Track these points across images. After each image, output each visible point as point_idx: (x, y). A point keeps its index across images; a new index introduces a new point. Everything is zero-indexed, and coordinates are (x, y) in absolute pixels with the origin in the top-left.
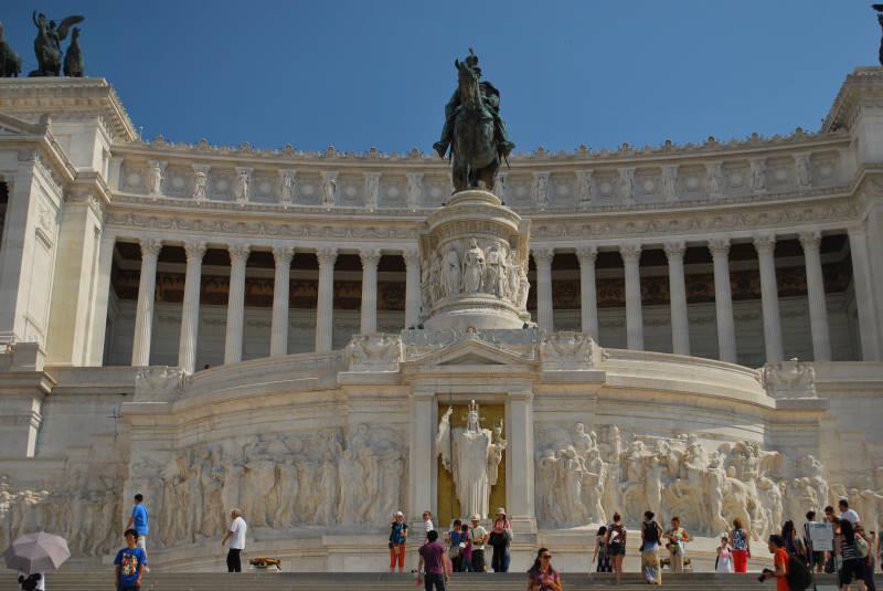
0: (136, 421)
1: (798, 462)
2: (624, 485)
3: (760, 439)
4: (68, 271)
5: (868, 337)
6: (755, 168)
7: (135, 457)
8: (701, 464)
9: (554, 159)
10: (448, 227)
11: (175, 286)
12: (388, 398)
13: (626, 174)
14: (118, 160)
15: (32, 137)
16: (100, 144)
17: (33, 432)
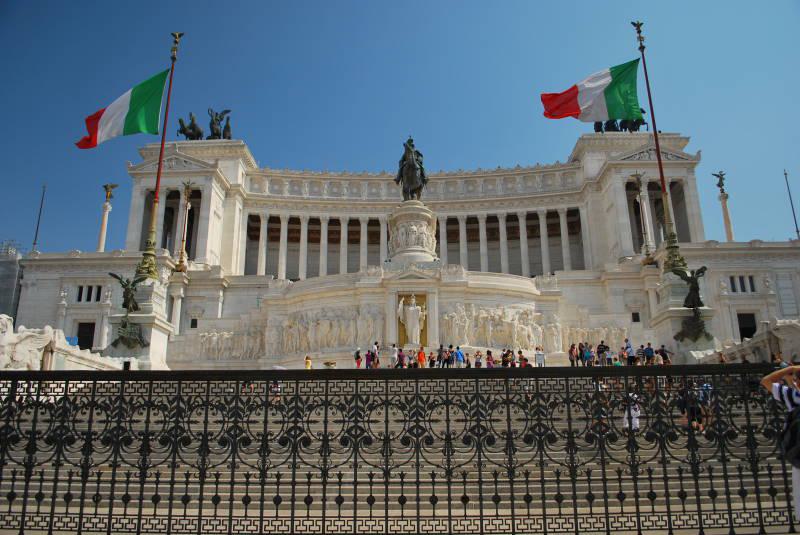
0: (271, 302)
1: (549, 318)
3: (533, 308)
4: (228, 229)
5: (587, 256)
6: (538, 179)
7: (270, 318)
8: (508, 320)
9: (447, 175)
10: (401, 216)
11: (276, 234)
12: (377, 293)
13: (480, 181)
14: (249, 178)
15: (211, 170)
16: (241, 170)
17: (220, 304)
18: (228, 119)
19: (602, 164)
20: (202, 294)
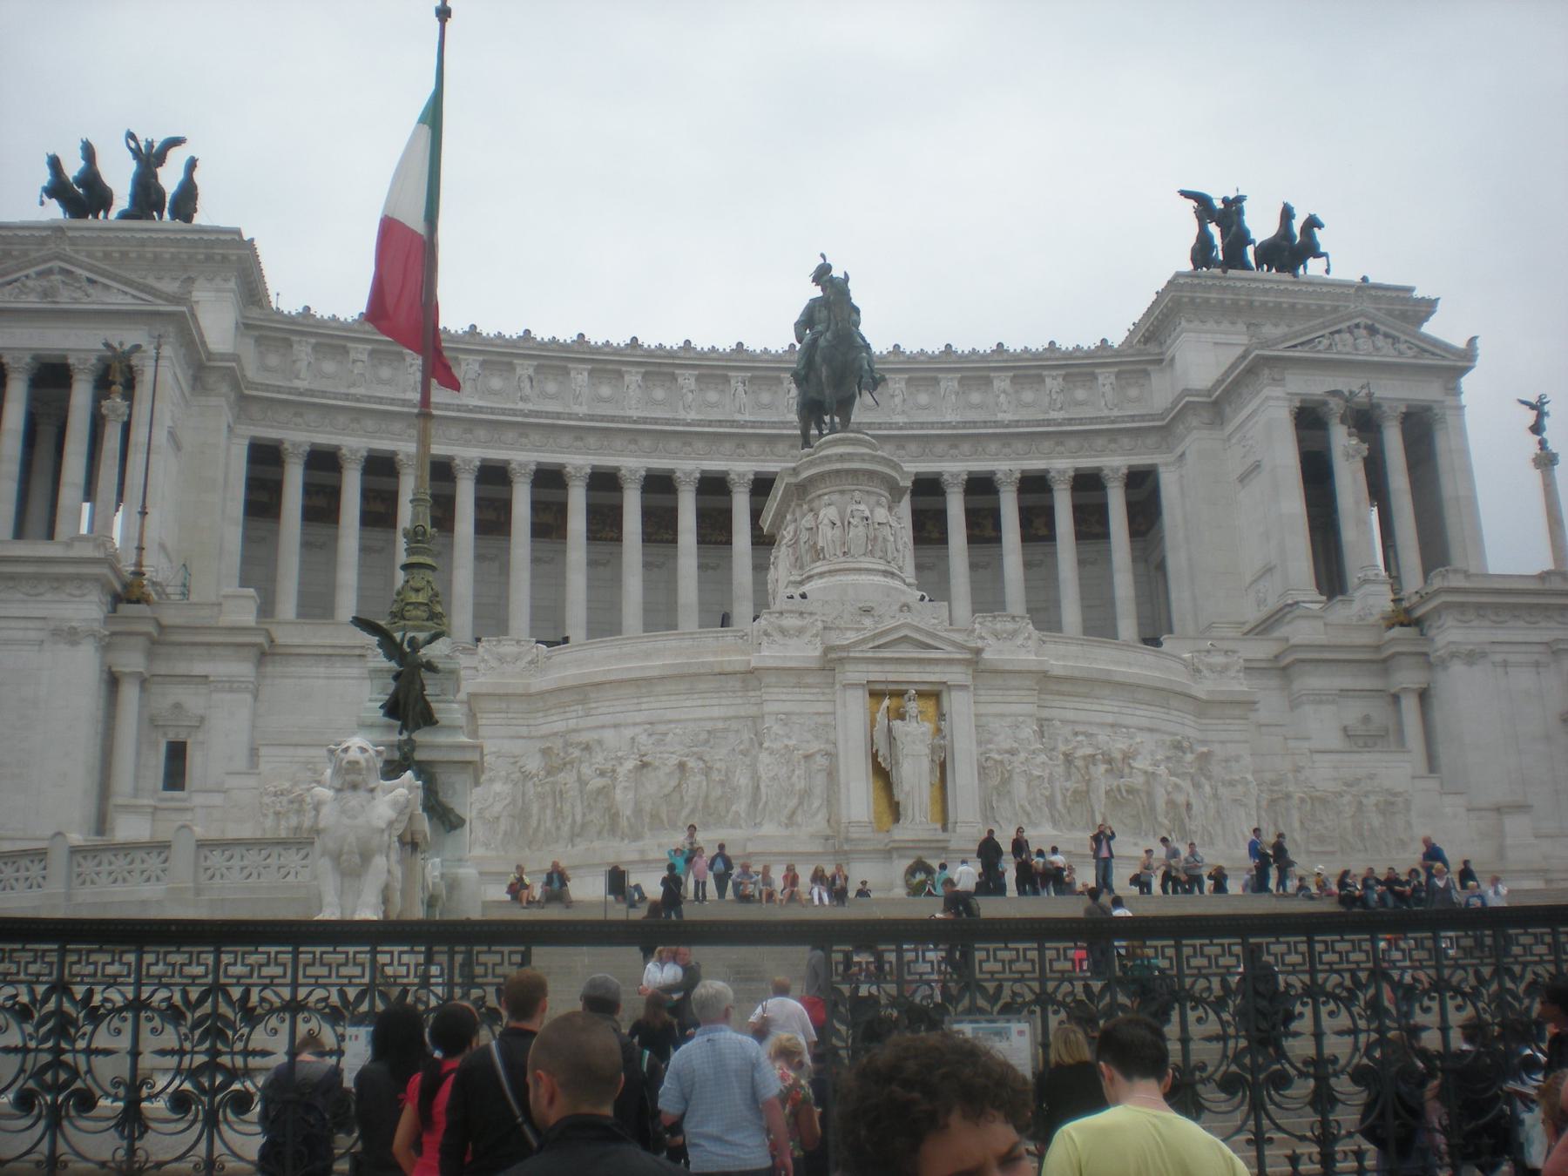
2: (1068, 784)
5: (1180, 597)
8: (1139, 764)
10: (822, 476)
18: (192, 165)
19: (1229, 356)
20: (199, 668)
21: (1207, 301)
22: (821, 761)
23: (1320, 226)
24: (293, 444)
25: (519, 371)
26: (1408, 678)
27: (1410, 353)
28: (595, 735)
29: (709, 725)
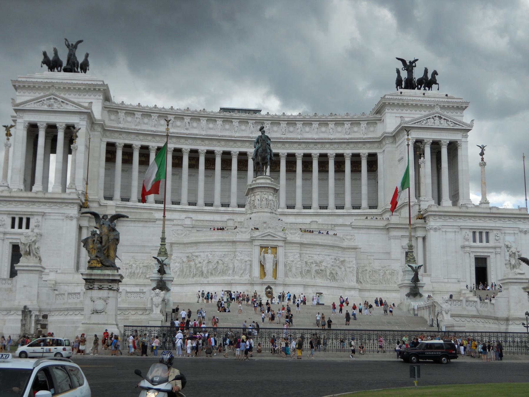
8: (323, 264)
10: (257, 187)
18: (87, 55)
21: (394, 103)
22: (249, 262)
23: (437, 74)
24: (119, 144)
25: (185, 120)
26: (420, 233)
27: (452, 125)
28: (199, 254)
29: (224, 253)
